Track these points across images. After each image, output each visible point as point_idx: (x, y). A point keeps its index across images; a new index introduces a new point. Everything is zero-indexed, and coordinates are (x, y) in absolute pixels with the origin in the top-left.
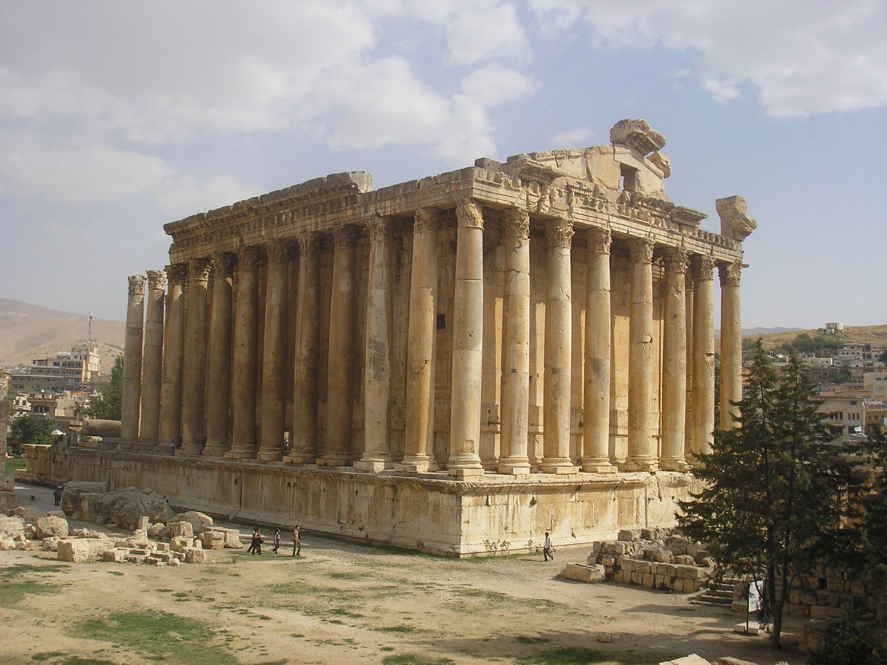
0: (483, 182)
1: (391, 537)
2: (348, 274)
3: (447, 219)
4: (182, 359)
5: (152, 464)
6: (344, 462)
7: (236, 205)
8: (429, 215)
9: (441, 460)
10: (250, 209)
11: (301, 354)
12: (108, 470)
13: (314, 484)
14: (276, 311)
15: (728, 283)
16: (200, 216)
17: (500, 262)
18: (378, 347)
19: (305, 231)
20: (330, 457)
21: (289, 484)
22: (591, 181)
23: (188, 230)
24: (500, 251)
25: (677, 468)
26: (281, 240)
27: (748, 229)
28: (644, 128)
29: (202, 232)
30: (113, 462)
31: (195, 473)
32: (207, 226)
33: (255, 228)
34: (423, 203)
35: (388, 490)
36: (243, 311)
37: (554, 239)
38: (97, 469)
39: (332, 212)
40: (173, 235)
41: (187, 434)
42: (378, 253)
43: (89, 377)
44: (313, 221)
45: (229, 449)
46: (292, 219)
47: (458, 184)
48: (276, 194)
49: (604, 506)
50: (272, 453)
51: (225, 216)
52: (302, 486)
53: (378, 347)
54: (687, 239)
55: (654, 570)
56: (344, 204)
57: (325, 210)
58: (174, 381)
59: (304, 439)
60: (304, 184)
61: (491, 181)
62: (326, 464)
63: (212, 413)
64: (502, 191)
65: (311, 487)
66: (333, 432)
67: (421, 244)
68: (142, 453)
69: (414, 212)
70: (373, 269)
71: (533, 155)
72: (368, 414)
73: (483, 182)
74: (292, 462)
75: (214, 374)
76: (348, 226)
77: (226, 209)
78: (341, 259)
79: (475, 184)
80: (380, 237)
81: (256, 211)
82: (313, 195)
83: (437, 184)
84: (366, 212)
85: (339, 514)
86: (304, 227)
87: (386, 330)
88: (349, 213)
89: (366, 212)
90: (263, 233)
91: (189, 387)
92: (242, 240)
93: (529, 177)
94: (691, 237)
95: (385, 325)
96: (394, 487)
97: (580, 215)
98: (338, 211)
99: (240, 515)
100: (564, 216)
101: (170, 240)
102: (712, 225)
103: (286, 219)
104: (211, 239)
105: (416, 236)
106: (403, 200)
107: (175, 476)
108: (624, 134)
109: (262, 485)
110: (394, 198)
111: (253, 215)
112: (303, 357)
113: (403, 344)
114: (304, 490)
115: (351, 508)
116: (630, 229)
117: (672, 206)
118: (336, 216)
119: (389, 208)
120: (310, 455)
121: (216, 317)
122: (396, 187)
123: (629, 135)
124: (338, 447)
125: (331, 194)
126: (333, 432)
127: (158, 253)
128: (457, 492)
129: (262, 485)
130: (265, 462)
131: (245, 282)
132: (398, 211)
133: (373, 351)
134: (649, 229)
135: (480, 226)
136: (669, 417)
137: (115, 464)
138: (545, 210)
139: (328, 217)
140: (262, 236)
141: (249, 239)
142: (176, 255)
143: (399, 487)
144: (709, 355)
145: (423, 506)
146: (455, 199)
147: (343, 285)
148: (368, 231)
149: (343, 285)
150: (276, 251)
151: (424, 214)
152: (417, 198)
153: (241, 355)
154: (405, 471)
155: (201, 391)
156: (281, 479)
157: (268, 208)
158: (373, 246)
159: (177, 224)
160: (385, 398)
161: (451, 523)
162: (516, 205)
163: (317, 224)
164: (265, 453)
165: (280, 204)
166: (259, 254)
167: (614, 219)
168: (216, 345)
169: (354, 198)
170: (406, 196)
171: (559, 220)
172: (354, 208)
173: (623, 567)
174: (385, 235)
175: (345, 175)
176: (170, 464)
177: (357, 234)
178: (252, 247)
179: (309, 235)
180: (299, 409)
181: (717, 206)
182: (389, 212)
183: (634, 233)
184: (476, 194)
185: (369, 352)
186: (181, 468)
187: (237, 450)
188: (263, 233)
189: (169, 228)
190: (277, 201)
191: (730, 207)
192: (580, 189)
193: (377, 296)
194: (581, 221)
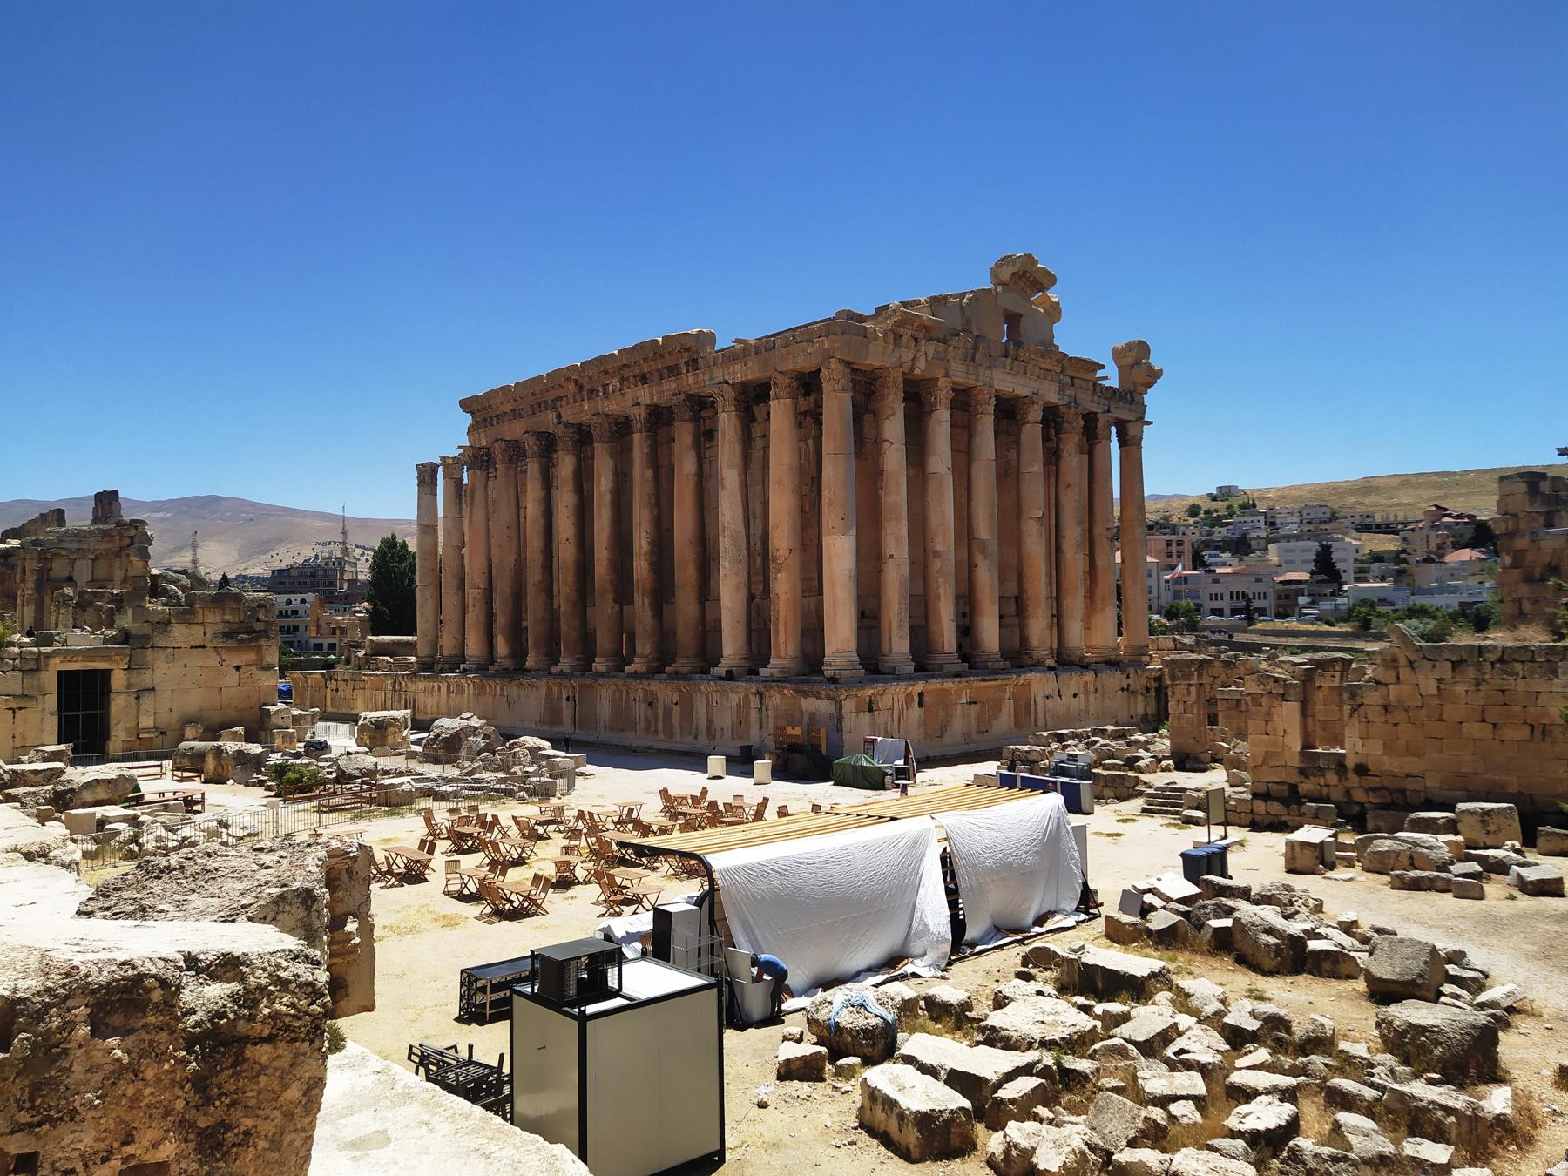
2: (693, 453)
3: (808, 384)
4: (490, 560)
10: (568, 379)
14: (607, 498)
15: (1131, 444)
16: (505, 389)
17: (868, 432)
20: (682, 664)
24: (868, 417)
26: (607, 415)
29: (508, 408)
35: (754, 702)
36: (565, 501)
38: (389, 695)
40: (472, 413)
41: (502, 648)
42: (727, 423)
43: (345, 586)
49: (997, 706)
62: (677, 673)
65: (661, 700)
66: (685, 633)
67: (780, 413)
75: (534, 576)
76: (689, 397)
78: (684, 434)
86: (635, 400)
92: (559, 416)
93: (901, 331)
95: (740, 510)
97: (960, 373)
100: (940, 374)
101: (468, 419)
102: (1111, 377)
108: (1006, 275)
113: (759, 531)
115: (710, 722)
126: (685, 633)
127: (451, 436)
130: (602, 675)
131: (566, 466)
137: (411, 687)
138: (921, 368)
139: (665, 387)
140: (582, 411)
141: (569, 414)
147: (686, 466)
149: (686, 466)
151: (780, 379)
153: (566, 551)
155: (518, 596)
160: (743, 594)
164: (600, 665)
169: (695, 361)
177: (701, 406)
180: (642, 608)
182: (739, 378)
189: (466, 405)
193: (729, 476)
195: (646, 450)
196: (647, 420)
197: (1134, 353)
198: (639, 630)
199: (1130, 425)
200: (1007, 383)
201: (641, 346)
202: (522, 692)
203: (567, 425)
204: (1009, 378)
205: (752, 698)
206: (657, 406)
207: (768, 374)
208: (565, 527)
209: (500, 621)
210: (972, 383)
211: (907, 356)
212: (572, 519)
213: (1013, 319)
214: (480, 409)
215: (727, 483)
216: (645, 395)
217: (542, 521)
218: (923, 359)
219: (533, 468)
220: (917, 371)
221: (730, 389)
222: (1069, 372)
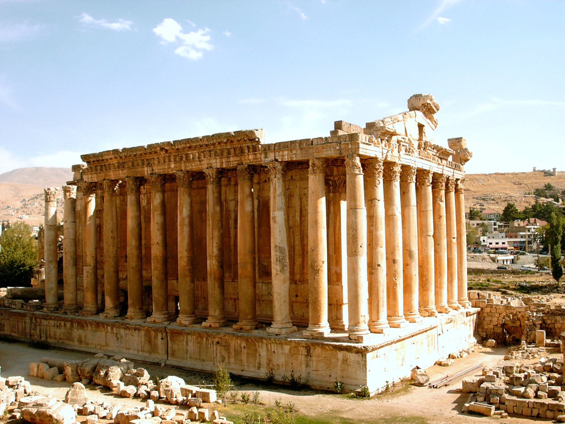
0: (364, 143)
1: (308, 381)
2: (250, 199)
5: (82, 325)
6: (254, 327)
7: (150, 146)
8: (321, 163)
9: (336, 326)
10: (162, 149)
11: (213, 252)
12: (38, 327)
13: (234, 343)
14: (187, 221)
16: (116, 151)
18: (281, 250)
19: (211, 167)
21: (213, 342)
22: (406, 135)
23: (102, 160)
25: (444, 311)
26: (188, 172)
27: (469, 158)
28: (431, 100)
29: (115, 162)
30: (43, 321)
31: (122, 332)
32: (121, 158)
33: (164, 162)
34: (316, 155)
35: (303, 351)
36: (156, 220)
38: (28, 325)
39: (236, 155)
40: (88, 162)
44: (218, 161)
45: (148, 314)
46: (199, 158)
47: (347, 144)
48: (188, 141)
50: (190, 319)
51: (139, 153)
52: (224, 344)
53: (281, 250)
54: (445, 168)
55: (531, 405)
56: (247, 151)
57: (229, 153)
58: (92, 265)
59: (218, 310)
60: (213, 136)
61: (367, 142)
62: (241, 329)
63: (132, 288)
68: (70, 316)
69: (307, 162)
70: (274, 198)
72: (275, 296)
73: (364, 143)
74: (210, 326)
76: (249, 166)
77: (141, 148)
79: (361, 145)
80: (279, 176)
81: (166, 151)
82: (219, 143)
83: (329, 143)
84: (266, 157)
85: (259, 364)
86: (210, 164)
87: (286, 239)
88: (251, 157)
89: (266, 157)
90: (173, 166)
91: (108, 269)
94: (447, 166)
96: (308, 349)
98: (241, 155)
99: (168, 362)
100: (397, 161)
103: (193, 158)
104: (123, 167)
105: (311, 177)
106: (299, 152)
107: (104, 333)
108: (419, 104)
109: (187, 342)
110: (291, 151)
111: (164, 152)
112: (214, 254)
114: (227, 347)
115: (269, 361)
116: (423, 165)
117: (442, 149)
118: (238, 159)
119: (286, 156)
120: (223, 321)
121: (131, 222)
122: (292, 142)
124: (250, 317)
125: (234, 143)
128: (363, 352)
129: (187, 342)
130: (186, 326)
131: (157, 199)
132: (294, 159)
133: (278, 253)
135: (362, 173)
136: (439, 280)
137: (45, 322)
138: (389, 159)
139: (232, 159)
140: (172, 167)
141: (158, 169)
142: (90, 176)
143: (312, 347)
144: (454, 238)
145: (333, 360)
146: (344, 154)
148: (269, 171)
150: (185, 179)
151: (317, 162)
152: (311, 151)
153: (156, 250)
154: (312, 335)
156: (205, 339)
157: (177, 149)
158: (274, 181)
159: (94, 155)
161: (358, 372)
163: (222, 163)
164: (183, 319)
165: (190, 147)
166: (167, 179)
168: (131, 242)
170: (301, 149)
171: (394, 164)
172: (256, 154)
173: (507, 403)
174: (282, 174)
175: (252, 132)
176: (98, 325)
177: (256, 171)
178: (161, 175)
179: (215, 170)
181: (449, 143)
182: (286, 159)
183: (426, 167)
184: (361, 152)
185: (274, 254)
186: (109, 328)
187: (157, 316)
188: (173, 166)
189: (84, 158)
190: (188, 145)
192: (405, 142)
195: (216, 195)
196: (217, 177)
198: (211, 299)
201: (219, 135)
202: (127, 332)
203: (160, 175)
205: (301, 348)
206: (223, 169)
207: (306, 158)
208: (156, 236)
209: (108, 287)
211: (385, 151)
212: (161, 231)
213: (421, 127)
214: (95, 161)
215: (278, 219)
216: (216, 163)
217: (137, 230)
219: (131, 199)
221: (279, 164)
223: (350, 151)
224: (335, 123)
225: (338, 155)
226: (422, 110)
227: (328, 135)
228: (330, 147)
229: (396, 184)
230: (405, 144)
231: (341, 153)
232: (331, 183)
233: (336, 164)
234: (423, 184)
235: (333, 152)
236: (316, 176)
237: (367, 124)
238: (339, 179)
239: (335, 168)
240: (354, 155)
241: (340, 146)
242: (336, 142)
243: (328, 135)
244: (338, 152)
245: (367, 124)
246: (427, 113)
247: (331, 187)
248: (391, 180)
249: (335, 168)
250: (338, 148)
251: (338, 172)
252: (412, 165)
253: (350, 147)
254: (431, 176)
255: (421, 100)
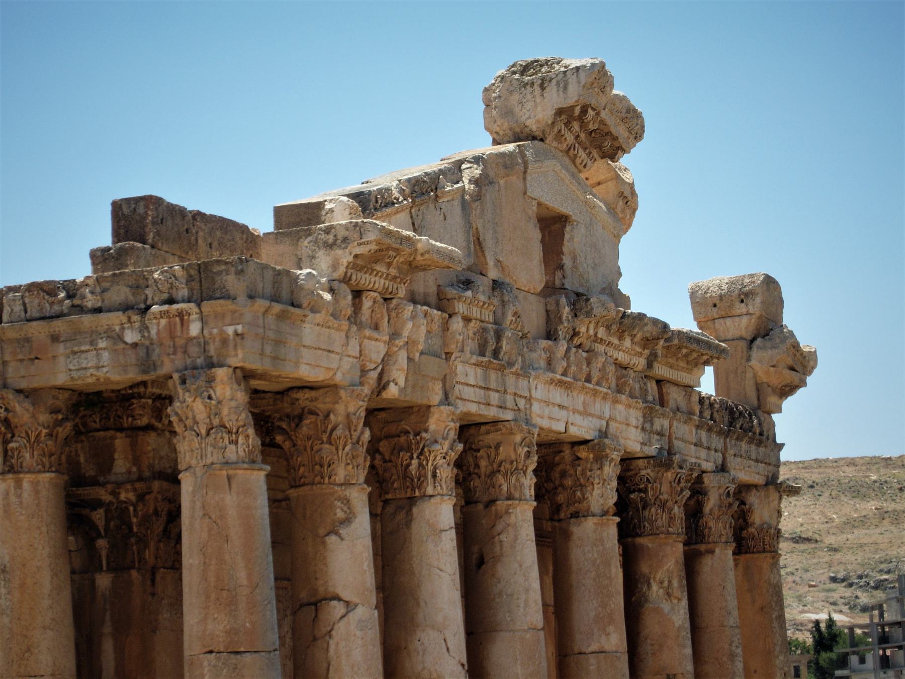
37: (406, 475)
47: (180, 314)
64: (310, 331)
71: (366, 202)
97: (472, 391)
123: (560, 112)
134: (606, 409)
162: (339, 377)
167: (540, 392)
183: (583, 428)
191: (741, 308)
194: (473, 408)
197: (755, 306)
199: (753, 499)
200: (558, 409)
204: (558, 395)
210: (492, 413)
211: (376, 350)
218: (402, 357)
220: (393, 391)
222: (661, 370)
223: (194, 350)
224: (117, 208)
225: (133, 375)
226: (559, 136)
227: (80, 270)
228: (93, 336)
229: (439, 513)
230: (475, 312)
231: (147, 364)
232: (98, 517)
233: (127, 422)
234: (576, 515)
235: (106, 355)
236: (19, 484)
237: (279, 212)
238: (141, 497)
239: (120, 442)
240: (221, 373)
241: (144, 328)
242: (126, 308)
243: (80, 270)
244: (132, 357)
245: (279, 212)
246: (582, 154)
247: (102, 543)
248: (412, 501)
249: (120, 442)
250: (131, 337)
251: (136, 461)
252: (509, 415)
253: (195, 329)
254: (611, 471)
255: (552, 91)
